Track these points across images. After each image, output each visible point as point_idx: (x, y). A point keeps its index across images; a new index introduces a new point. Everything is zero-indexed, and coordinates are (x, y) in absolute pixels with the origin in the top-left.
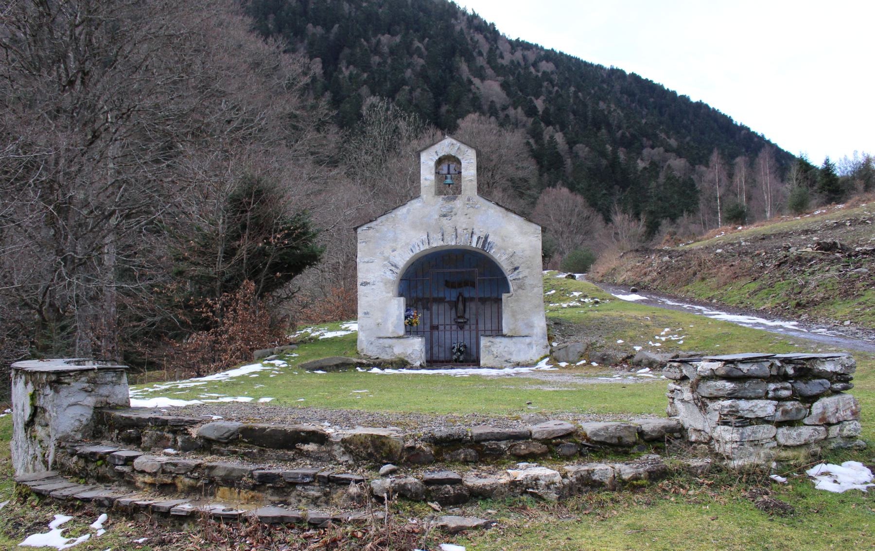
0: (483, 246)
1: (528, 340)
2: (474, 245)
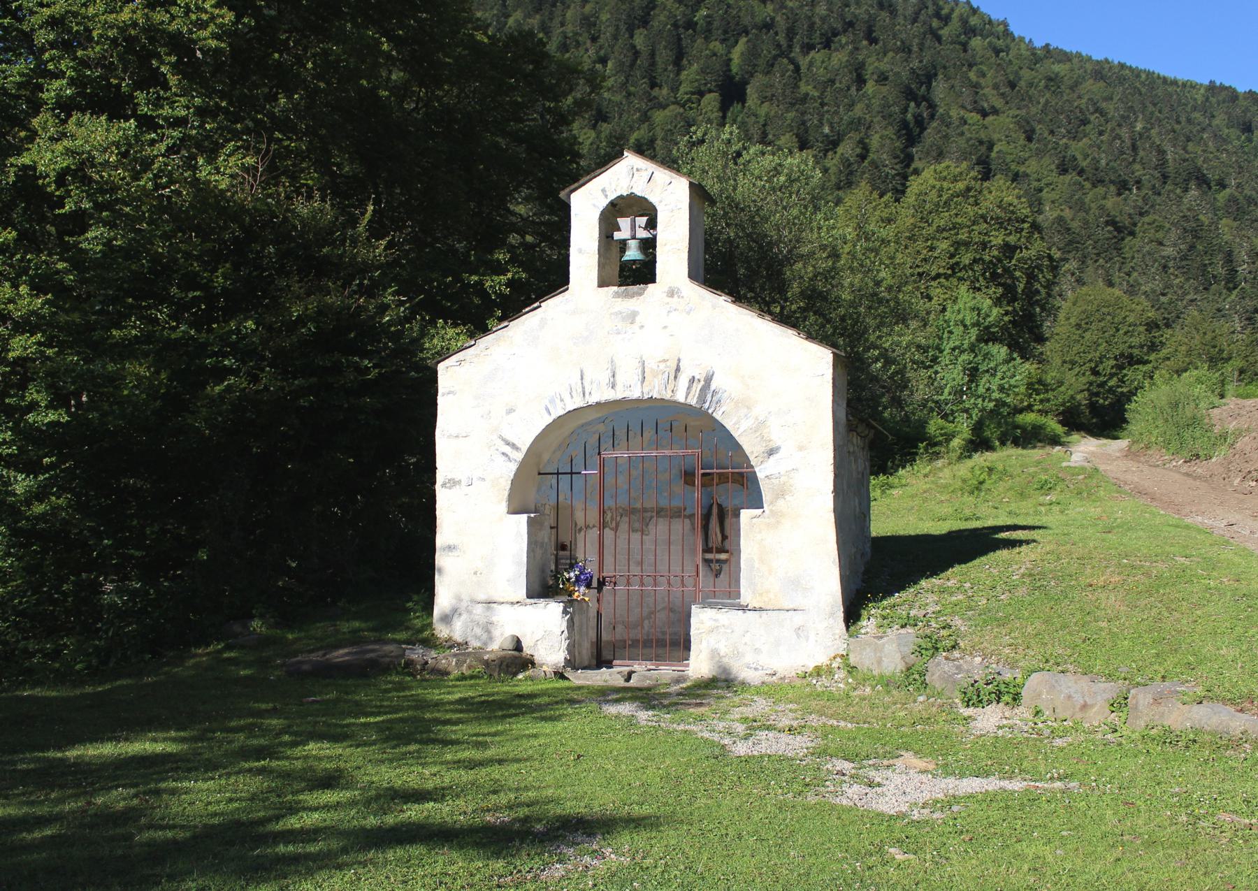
0: (702, 398)
1: (798, 619)
2: (680, 397)
